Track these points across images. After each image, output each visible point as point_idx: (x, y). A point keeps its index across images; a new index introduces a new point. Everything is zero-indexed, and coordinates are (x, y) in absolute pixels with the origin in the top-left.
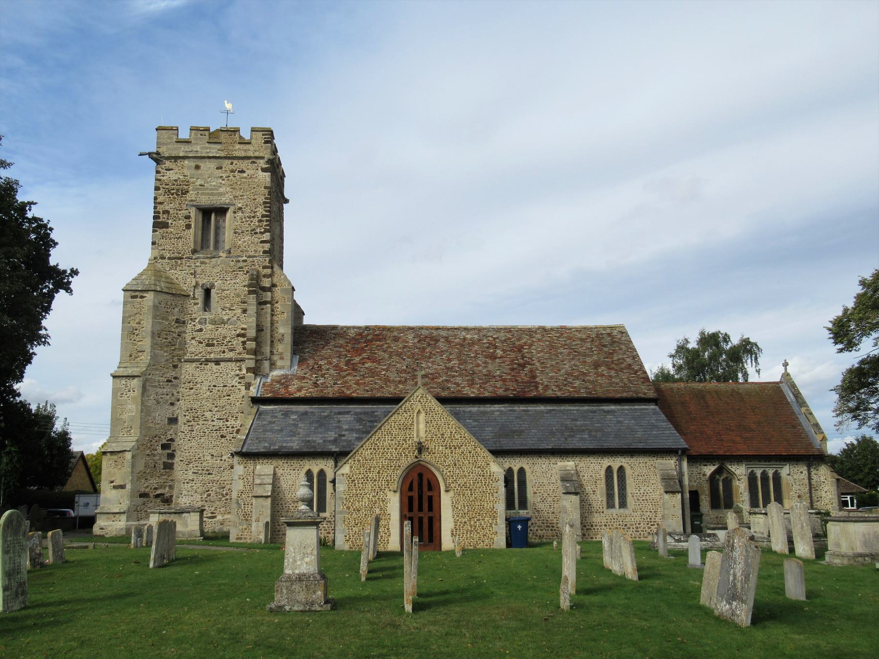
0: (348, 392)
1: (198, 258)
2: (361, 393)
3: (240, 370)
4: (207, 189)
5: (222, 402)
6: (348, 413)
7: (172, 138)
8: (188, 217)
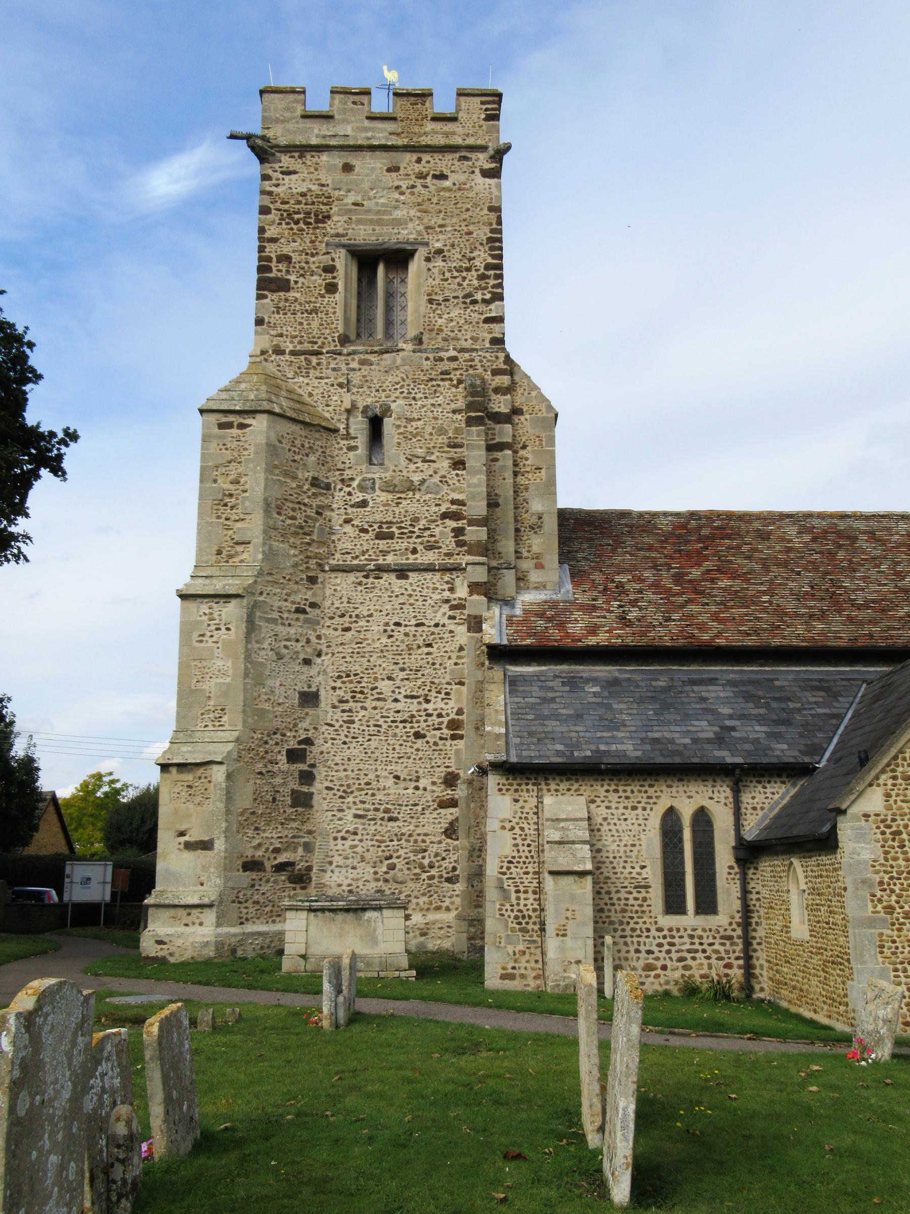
0: (706, 637)
1: (354, 353)
2: (729, 638)
3: (452, 590)
4: (368, 211)
5: (416, 659)
6: (712, 681)
7: (294, 111)
8: (330, 269)
